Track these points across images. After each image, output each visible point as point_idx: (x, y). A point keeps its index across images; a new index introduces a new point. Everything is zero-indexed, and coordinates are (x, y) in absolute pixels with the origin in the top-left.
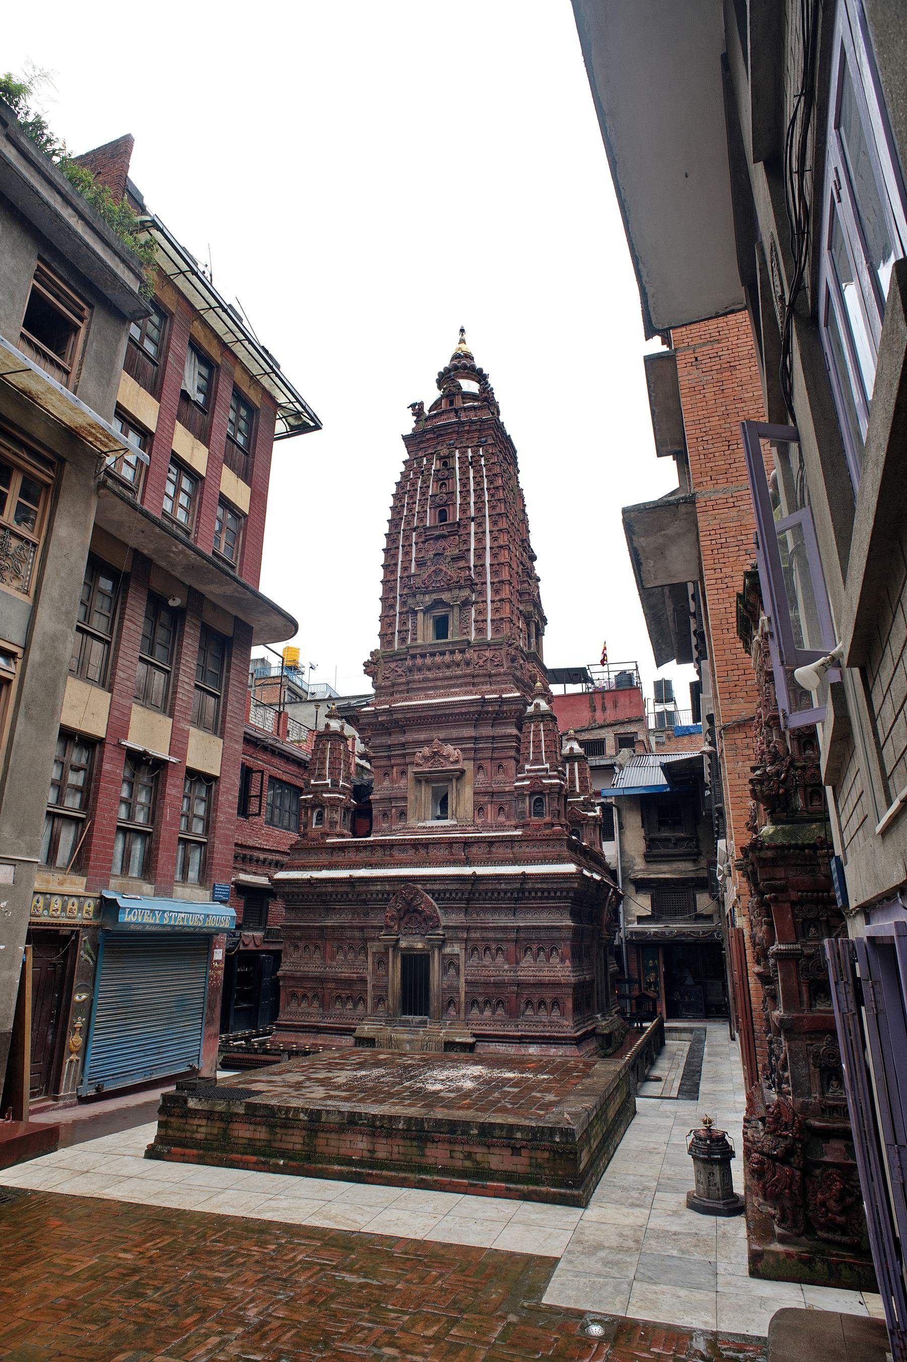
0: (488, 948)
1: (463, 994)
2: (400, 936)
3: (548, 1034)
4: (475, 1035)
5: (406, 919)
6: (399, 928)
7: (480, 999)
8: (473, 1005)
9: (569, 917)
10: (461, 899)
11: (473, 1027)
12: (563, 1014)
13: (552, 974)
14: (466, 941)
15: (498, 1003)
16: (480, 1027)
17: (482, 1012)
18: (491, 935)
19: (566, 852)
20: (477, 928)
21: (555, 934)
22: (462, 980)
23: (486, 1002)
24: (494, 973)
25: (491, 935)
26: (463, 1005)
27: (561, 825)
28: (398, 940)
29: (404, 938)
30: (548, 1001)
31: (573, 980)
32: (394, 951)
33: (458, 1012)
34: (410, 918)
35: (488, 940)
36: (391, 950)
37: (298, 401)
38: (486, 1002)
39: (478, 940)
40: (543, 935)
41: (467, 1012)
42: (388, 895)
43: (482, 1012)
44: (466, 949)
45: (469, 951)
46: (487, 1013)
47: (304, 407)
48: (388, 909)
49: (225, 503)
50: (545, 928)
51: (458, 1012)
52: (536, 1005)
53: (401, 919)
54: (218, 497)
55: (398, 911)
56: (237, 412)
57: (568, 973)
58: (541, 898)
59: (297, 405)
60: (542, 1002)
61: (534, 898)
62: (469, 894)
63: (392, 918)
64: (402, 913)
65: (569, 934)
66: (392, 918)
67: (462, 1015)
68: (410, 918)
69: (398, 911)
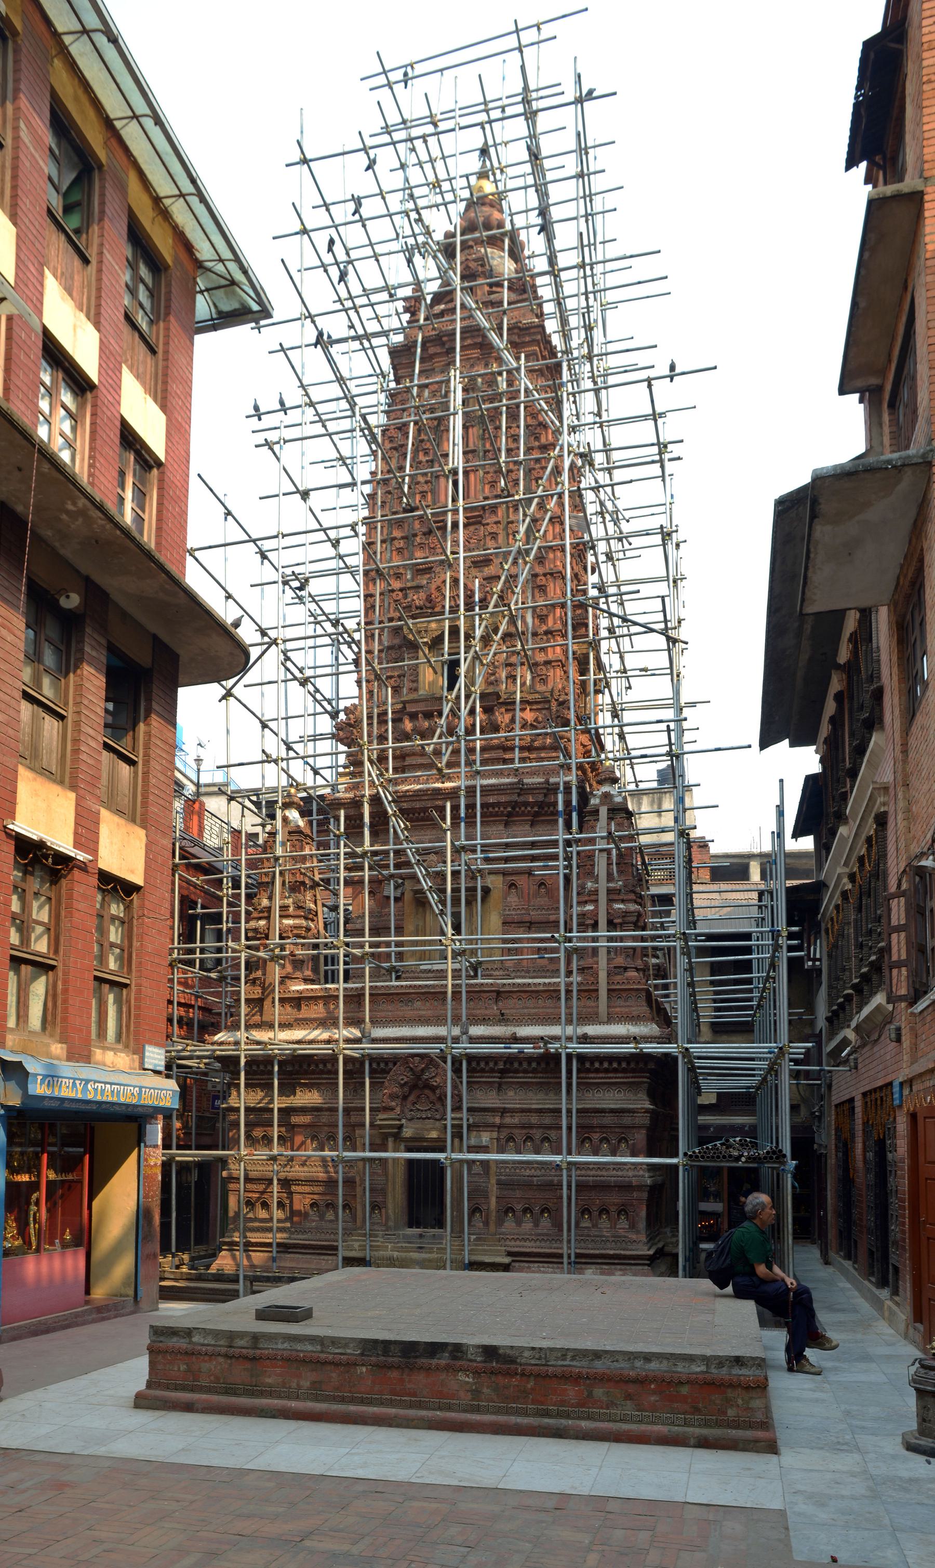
0: (529, 1138)
1: (493, 1201)
2: (404, 1121)
3: (612, 1252)
4: (510, 1254)
5: (412, 1098)
6: (402, 1111)
7: (518, 1207)
8: (506, 1212)
9: (645, 1097)
10: (492, 1071)
11: (508, 1243)
12: (633, 1226)
13: (620, 1173)
14: (500, 1127)
15: (542, 1212)
16: (518, 1243)
17: (519, 1223)
18: (534, 1119)
19: (644, 1009)
20: (513, 1111)
21: (627, 1120)
22: (493, 1181)
23: (525, 1210)
24: (538, 1173)
25: (534, 1119)
26: (494, 1214)
27: (637, 970)
28: (401, 1127)
29: (410, 1124)
30: (613, 1209)
31: (649, 1182)
32: (395, 1141)
33: (486, 1223)
34: (419, 1097)
35: (531, 1127)
36: (390, 1140)
37: (237, 259)
38: (525, 1210)
39: (516, 1127)
40: (608, 1120)
41: (500, 1222)
42: (386, 1064)
43: (519, 1223)
44: (498, 1139)
45: (503, 1142)
46: (527, 1225)
47: (245, 272)
48: (387, 1084)
49: (129, 439)
50: (612, 1111)
51: (486, 1223)
52: (596, 1214)
53: (405, 1098)
54: (118, 424)
55: (402, 1086)
56: (133, 266)
57: (641, 1173)
58: (606, 1071)
59: (233, 267)
60: (604, 1210)
61: (597, 1071)
62: (505, 1063)
63: (392, 1097)
64: (406, 1089)
65: (646, 1120)
66: (392, 1097)
67: (492, 1227)
68: (419, 1097)
69: (402, 1086)
